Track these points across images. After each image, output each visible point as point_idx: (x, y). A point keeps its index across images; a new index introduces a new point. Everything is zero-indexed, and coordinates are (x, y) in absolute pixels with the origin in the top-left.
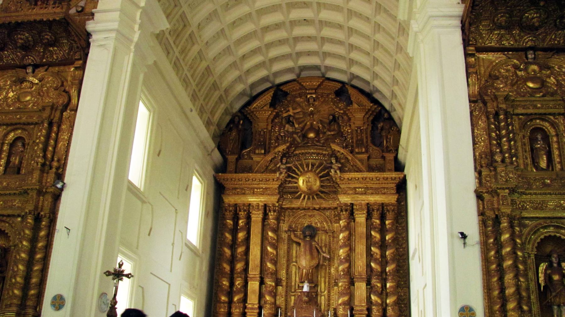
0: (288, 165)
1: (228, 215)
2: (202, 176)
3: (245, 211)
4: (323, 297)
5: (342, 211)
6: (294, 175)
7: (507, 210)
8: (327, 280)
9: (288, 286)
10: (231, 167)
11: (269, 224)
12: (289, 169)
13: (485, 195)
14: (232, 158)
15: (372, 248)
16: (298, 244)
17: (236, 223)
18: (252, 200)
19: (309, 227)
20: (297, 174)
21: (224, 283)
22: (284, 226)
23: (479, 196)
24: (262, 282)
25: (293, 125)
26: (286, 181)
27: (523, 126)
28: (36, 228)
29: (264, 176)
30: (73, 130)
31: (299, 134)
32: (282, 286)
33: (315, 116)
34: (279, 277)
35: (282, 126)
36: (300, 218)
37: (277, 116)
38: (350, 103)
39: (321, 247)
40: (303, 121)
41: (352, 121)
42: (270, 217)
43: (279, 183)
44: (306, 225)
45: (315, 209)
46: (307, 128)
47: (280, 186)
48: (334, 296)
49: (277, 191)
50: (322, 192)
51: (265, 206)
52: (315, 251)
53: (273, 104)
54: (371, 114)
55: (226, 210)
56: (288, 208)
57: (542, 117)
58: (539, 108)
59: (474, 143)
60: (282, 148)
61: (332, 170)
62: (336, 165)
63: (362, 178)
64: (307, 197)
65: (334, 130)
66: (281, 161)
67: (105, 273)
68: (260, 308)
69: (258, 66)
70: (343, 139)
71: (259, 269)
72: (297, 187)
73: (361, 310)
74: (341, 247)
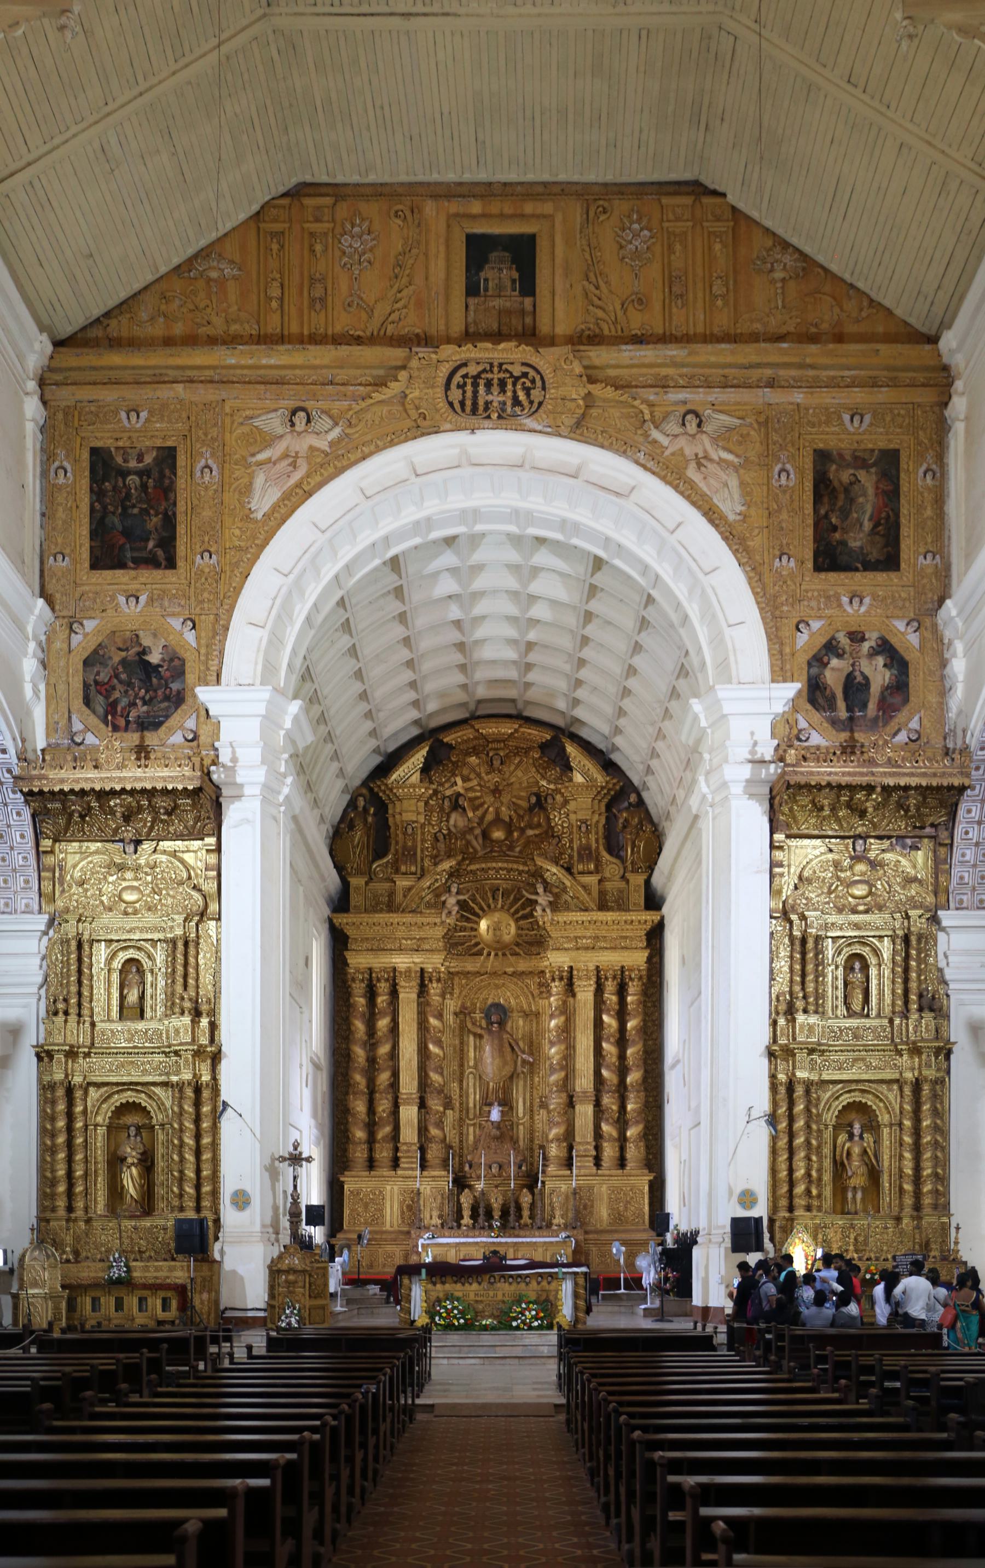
27: (839, 952)
57: (862, 941)
59: (772, 979)
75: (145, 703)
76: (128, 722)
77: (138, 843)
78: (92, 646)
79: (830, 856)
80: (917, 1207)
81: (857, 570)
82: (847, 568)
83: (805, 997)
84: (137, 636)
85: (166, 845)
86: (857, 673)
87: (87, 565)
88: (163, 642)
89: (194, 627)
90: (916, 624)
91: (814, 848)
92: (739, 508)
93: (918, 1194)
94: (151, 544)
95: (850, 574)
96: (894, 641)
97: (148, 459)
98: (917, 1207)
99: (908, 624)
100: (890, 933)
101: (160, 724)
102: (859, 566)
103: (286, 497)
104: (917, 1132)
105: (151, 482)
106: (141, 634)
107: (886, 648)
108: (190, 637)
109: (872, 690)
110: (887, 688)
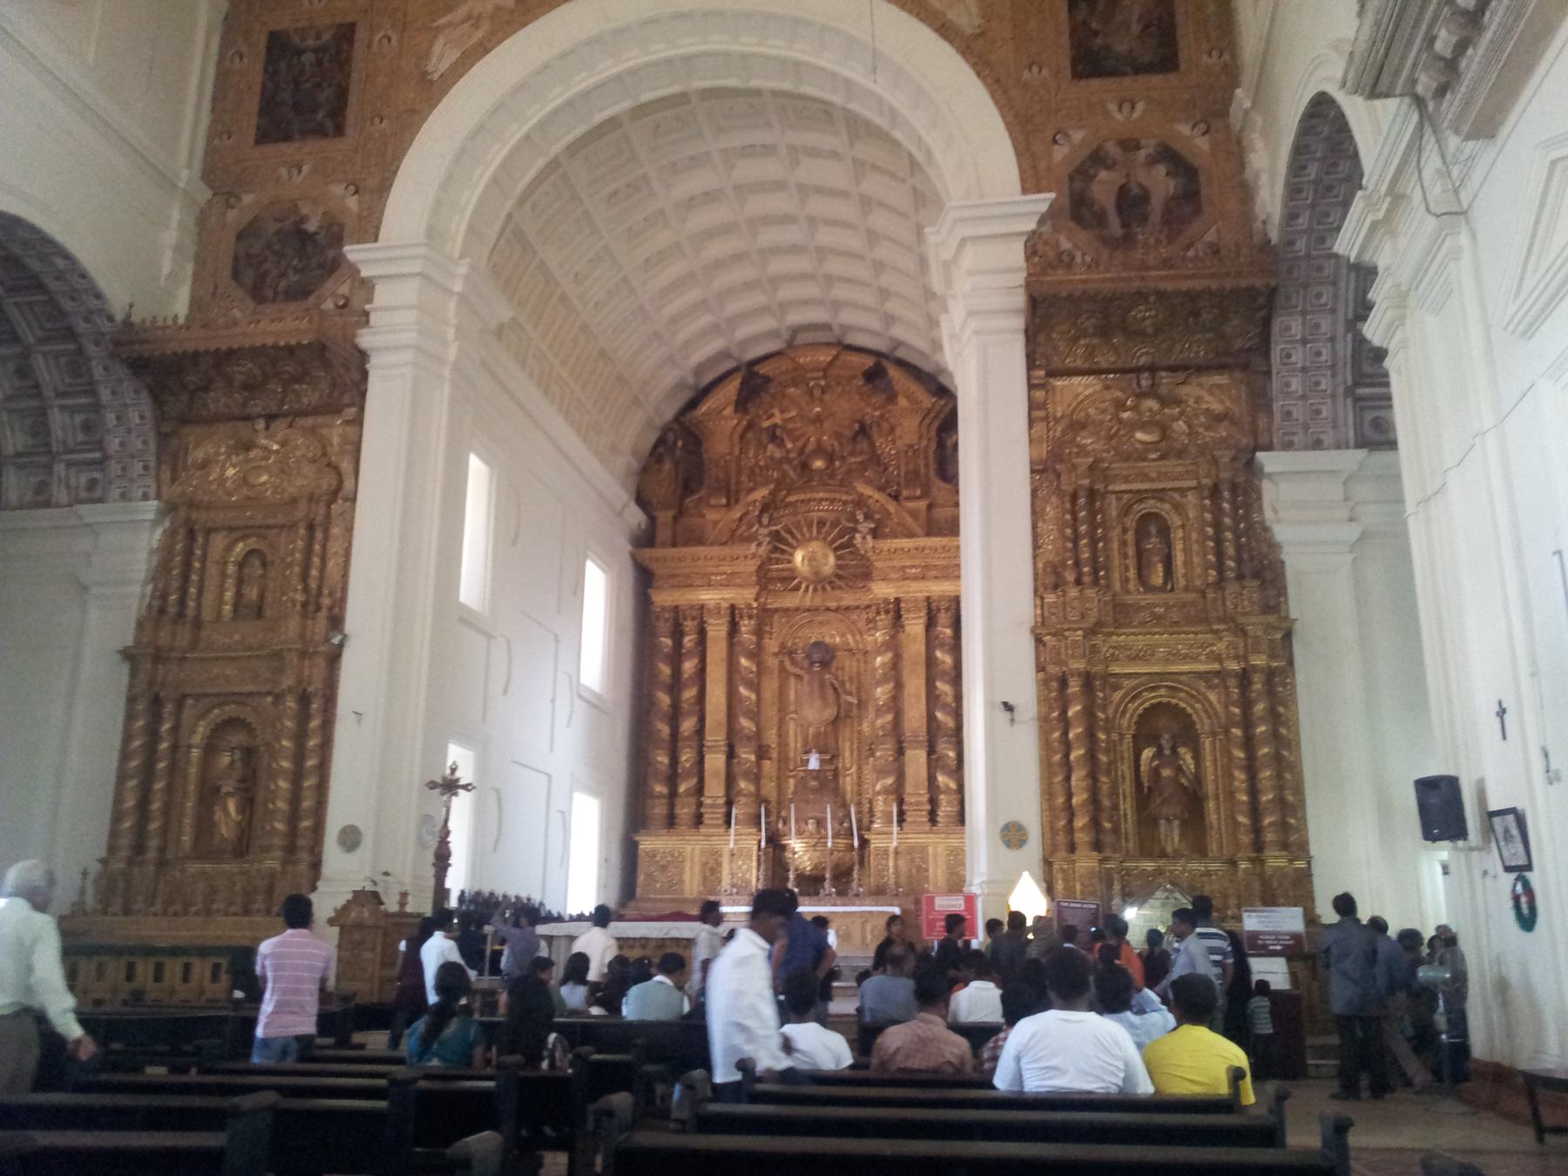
0: (773, 528)
1: (664, 627)
2: (605, 565)
3: (694, 619)
4: (848, 778)
5: (878, 613)
6: (785, 548)
7: (1078, 665)
8: (855, 746)
9: (783, 759)
10: (664, 533)
11: (740, 643)
12: (776, 536)
13: (1047, 638)
14: (665, 516)
15: (939, 684)
16: (798, 677)
17: (678, 643)
18: (708, 597)
19: (818, 645)
20: (790, 546)
21: (659, 759)
22: (771, 645)
23: (1039, 641)
24: (731, 755)
25: (781, 444)
26: (770, 559)
27: (1126, 511)
28: (303, 717)
29: (727, 551)
30: (351, 536)
31: (795, 463)
32: (770, 759)
33: (827, 424)
34: (765, 742)
35: (761, 447)
36: (801, 627)
37: (751, 426)
38: (892, 398)
39: (843, 683)
40: (802, 435)
41: (898, 432)
42: (743, 629)
43: (759, 563)
44: (812, 641)
45: (828, 609)
46: (811, 447)
47: (760, 568)
48: (869, 775)
49: (754, 578)
50: (839, 577)
51: (733, 608)
52: (831, 691)
53: (741, 404)
54: (934, 418)
55: (658, 619)
56: (777, 610)
57: (1159, 494)
58: (1153, 480)
59: (1036, 546)
60: (761, 493)
61: (858, 536)
62: (865, 524)
63: (917, 549)
64: (811, 588)
65: (862, 453)
66: (760, 522)
67: (427, 785)
68: (729, 804)
69: (705, 334)
70: (881, 469)
71: (724, 729)
72: (792, 570)
73: (918, 804)
74: (878, 684)
75: (297, 271)
76: (276, 293)
77: (270, 418)
78: (248, 217)
79: (1108, 395)
80: (1258, 846)
81: (1124, 74)
82: (1113, 73)
83: (1077, 564)
84: (296, 206)
85: (301, 422)
86: (1133, 185)
87: (252, 141)
88: (321, 210)
89: (356, 192)
90: (1202, 127)
91: (1087, 386)
92: (978, 21)
93: (1257, 830)
94: (320, 115)
95: (1118, 79)
96: (1177, 146)
97: (327, 36)
98: (1258, 846)
99: (1194, 127)
100: (1193, 483)
101: (310, 293)
102: (1128, 69)
103: (464, 55)
104: (1249, 743)
105: (327, 58)
106: (300, 203)
107: (1170, 156)
108: (352, 203)
109: (1153, 201)
110: (1173, 198)
